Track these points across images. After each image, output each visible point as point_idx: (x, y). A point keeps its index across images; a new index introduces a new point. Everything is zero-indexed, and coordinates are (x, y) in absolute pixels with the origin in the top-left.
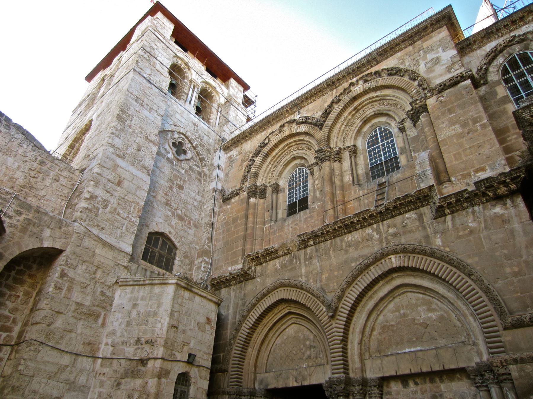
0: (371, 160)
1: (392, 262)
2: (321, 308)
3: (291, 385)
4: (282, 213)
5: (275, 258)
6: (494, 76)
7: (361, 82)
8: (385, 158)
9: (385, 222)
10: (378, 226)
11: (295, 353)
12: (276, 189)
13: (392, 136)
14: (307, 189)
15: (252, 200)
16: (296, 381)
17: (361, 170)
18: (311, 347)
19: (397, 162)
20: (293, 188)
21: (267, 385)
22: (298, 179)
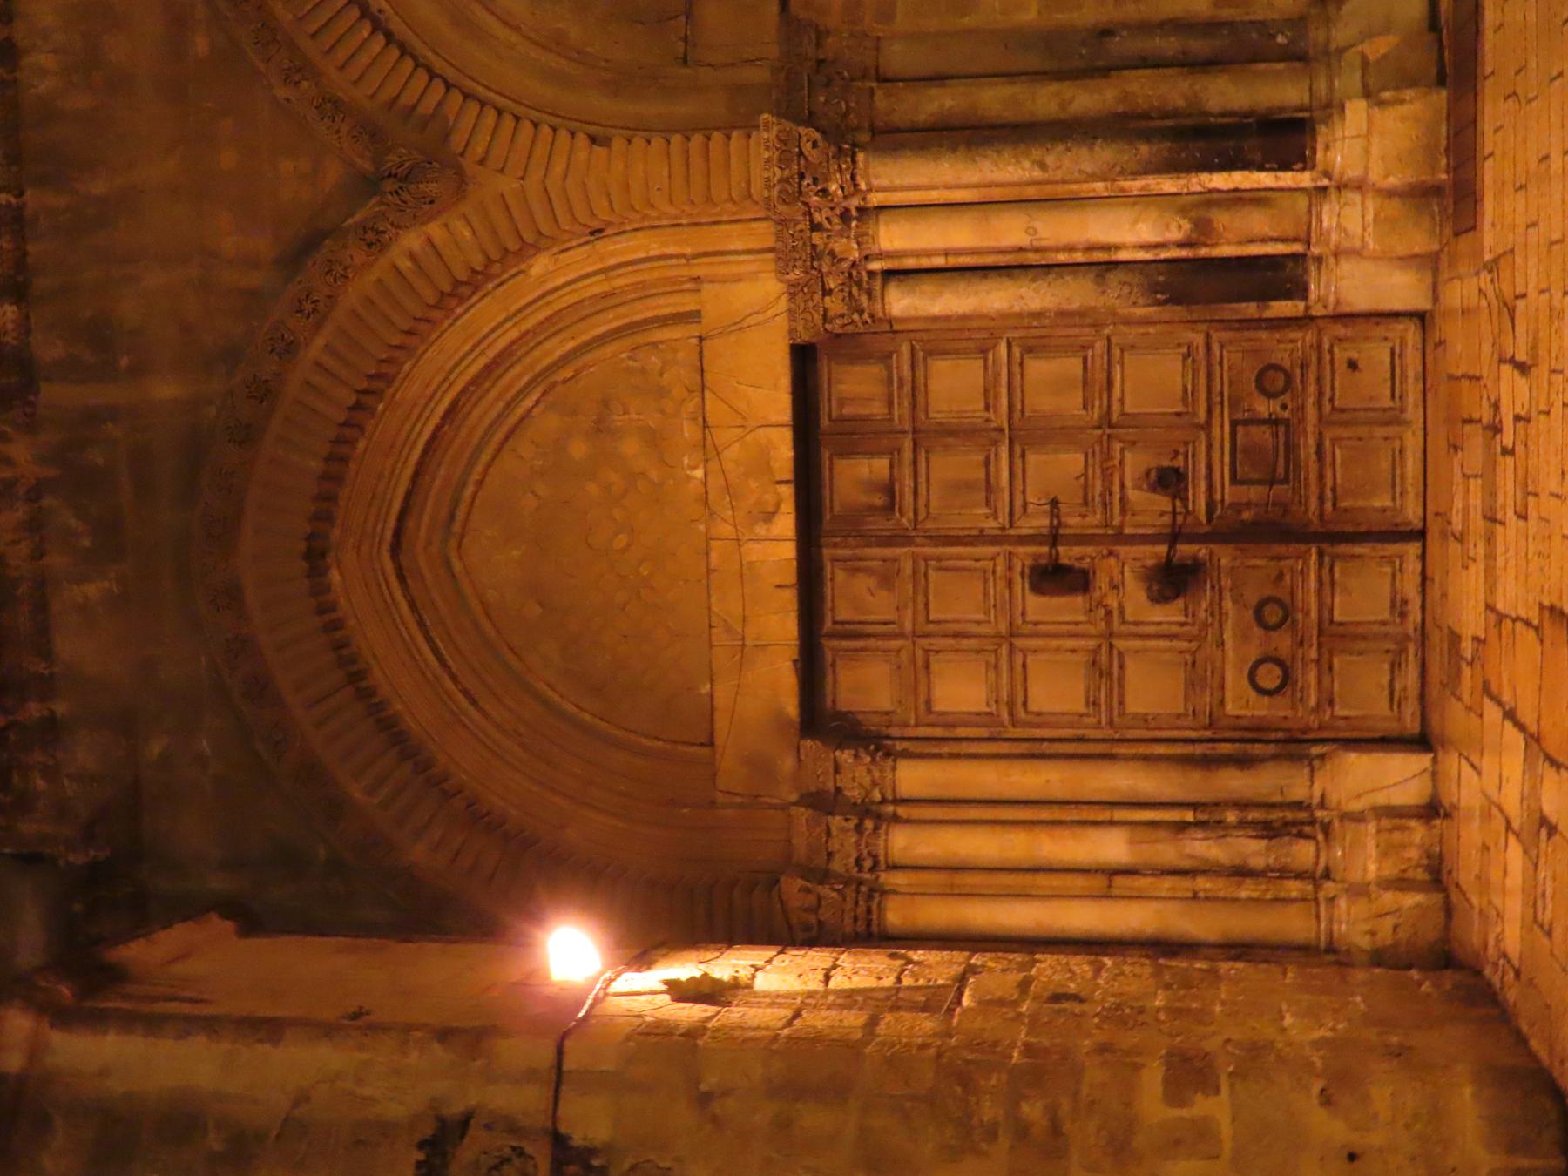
2: (405, 264)
3: (789, 551)
11: (622, 540)
16: (769, 517)
18: (601, 429)
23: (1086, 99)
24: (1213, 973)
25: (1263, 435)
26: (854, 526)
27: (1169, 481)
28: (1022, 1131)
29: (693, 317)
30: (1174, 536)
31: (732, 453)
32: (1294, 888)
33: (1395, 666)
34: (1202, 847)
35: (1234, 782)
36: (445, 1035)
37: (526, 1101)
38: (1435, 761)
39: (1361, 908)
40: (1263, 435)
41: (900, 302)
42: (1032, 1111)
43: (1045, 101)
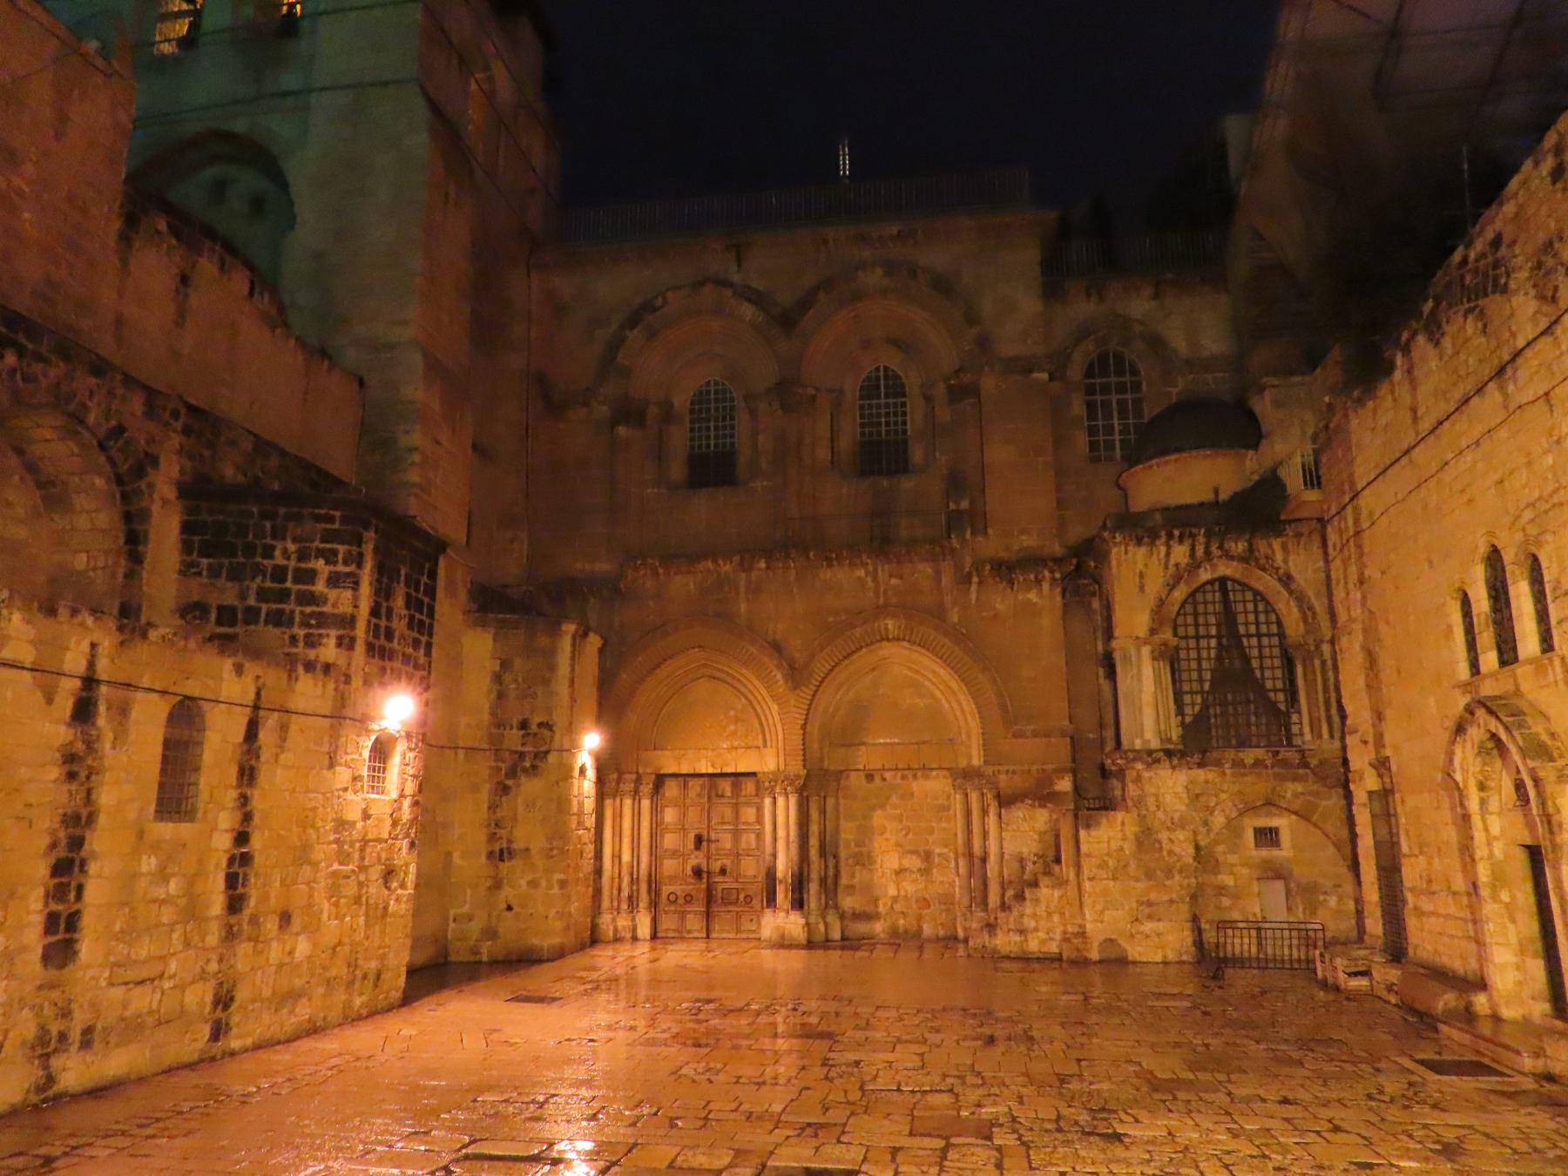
0: (862, 425)
1: (886, 629)
3: (704, 771)
4: (677, 471)
5: (689, 572)
6: (1075, 372)
7: (879, 271)
8: (888, 432)
9: (886, 566)
10: (876, 570)
12: (668, 415)
13: (904, 395)
14: (732, 436)
15: (622, 430)
17: (846, 442)
18: (737, 720)
19: (905, 451)
20: (700, 420)
21: (660, 769)
22: (712, 405)
23: (814, 853)
24: (588, 886)
25: (735, 896)
26: (713, 787)
27: (723, 872)
28: (551, 850)
29: (765, 746)
30: (708, 872)
31: (729, 756)
32: (615, 904)
33: (674, 931)
34: (626, 880)
35: (644, 888)
36: (571, 724)
37: (556, 744)
38: (645, 940)
39: (609, 921)
40: (734, 897)
41: (768, 801)
42: (555, 852)
43: (814, 842)
